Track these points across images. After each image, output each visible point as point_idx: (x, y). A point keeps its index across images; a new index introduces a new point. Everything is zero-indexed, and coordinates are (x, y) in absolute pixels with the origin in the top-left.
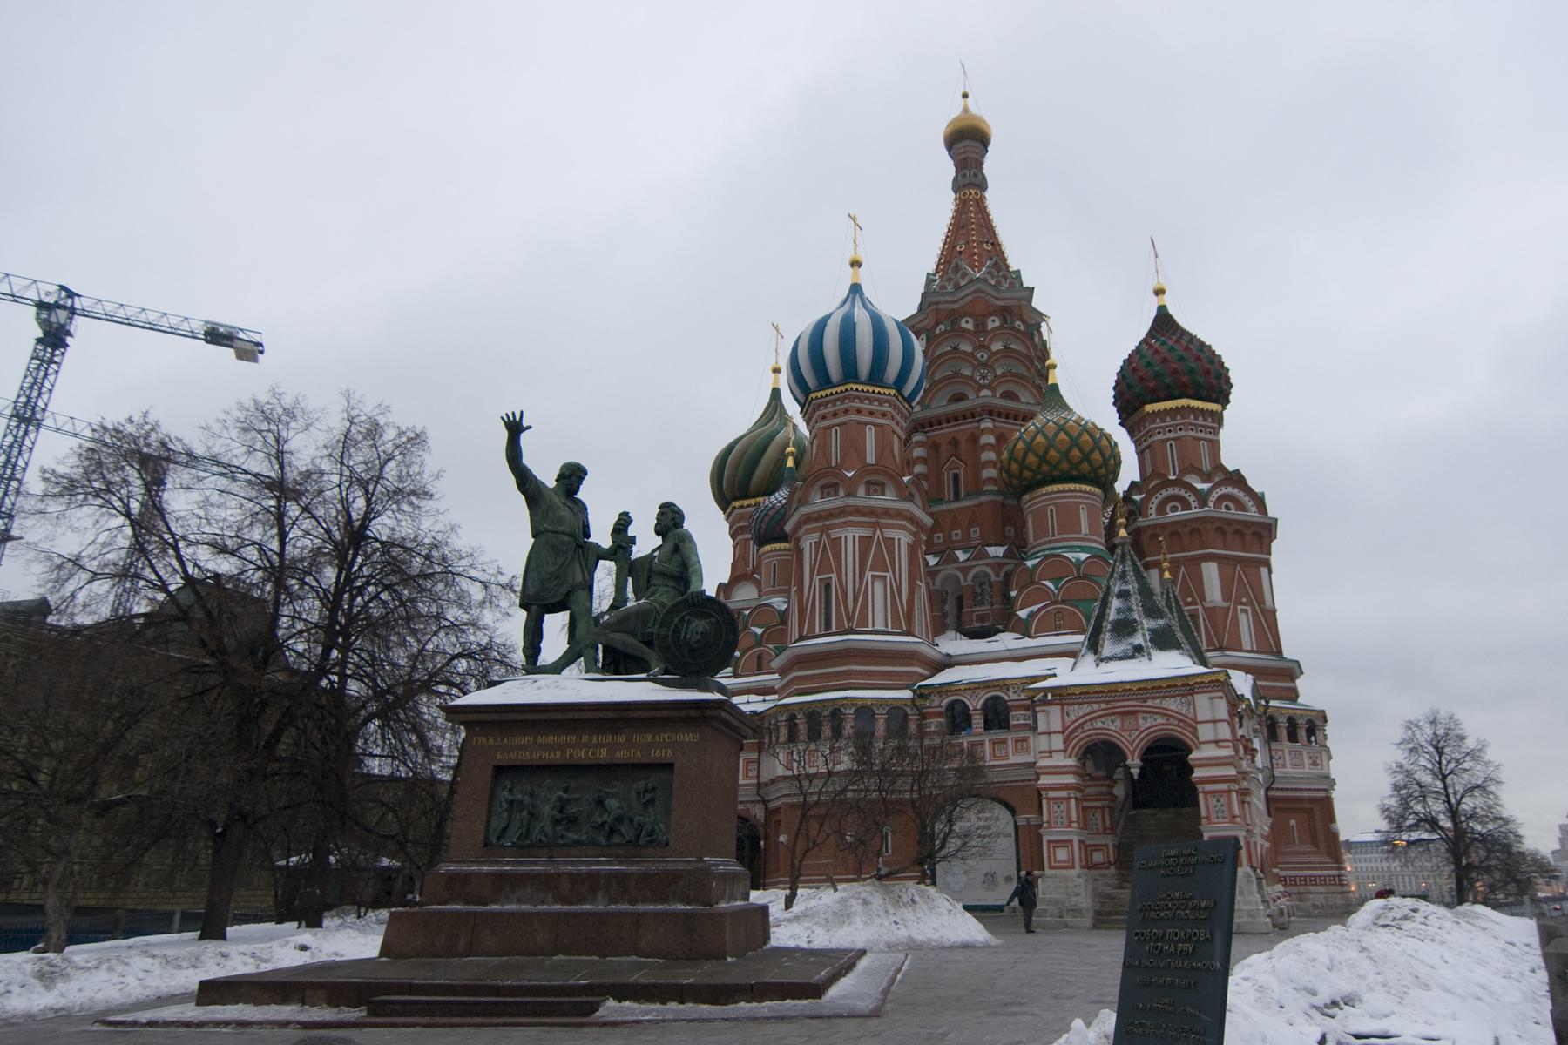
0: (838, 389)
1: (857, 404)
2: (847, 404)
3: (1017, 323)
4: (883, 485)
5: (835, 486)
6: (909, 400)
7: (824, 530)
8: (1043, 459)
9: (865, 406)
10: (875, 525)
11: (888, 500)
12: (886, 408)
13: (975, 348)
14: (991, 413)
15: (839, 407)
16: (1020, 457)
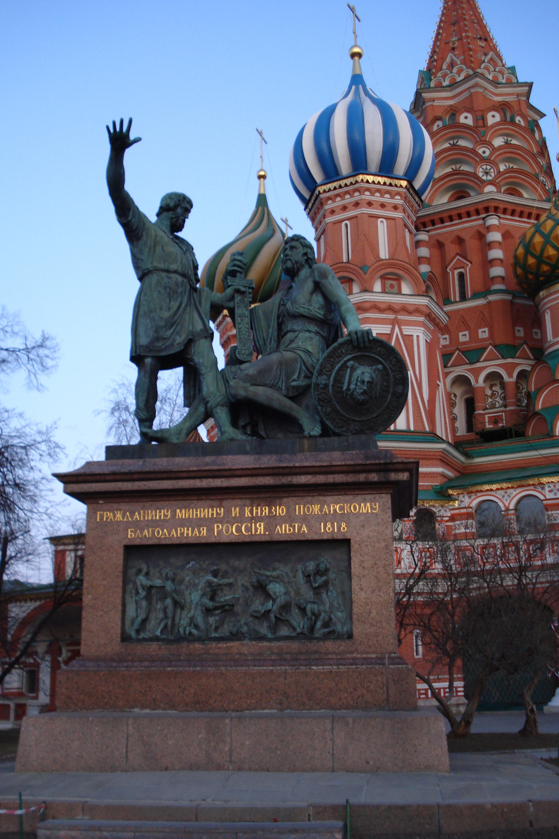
0: (348, 181)
1: (367, 196)
3: (518, 119)
4: (398, 279)
6: (418, 194)
9: (377, 197)
10: (394, 323)
12: (398, 200)
13: (476, 143)
14: (496, 209)
15: (348, 199)
16: (538, 253)
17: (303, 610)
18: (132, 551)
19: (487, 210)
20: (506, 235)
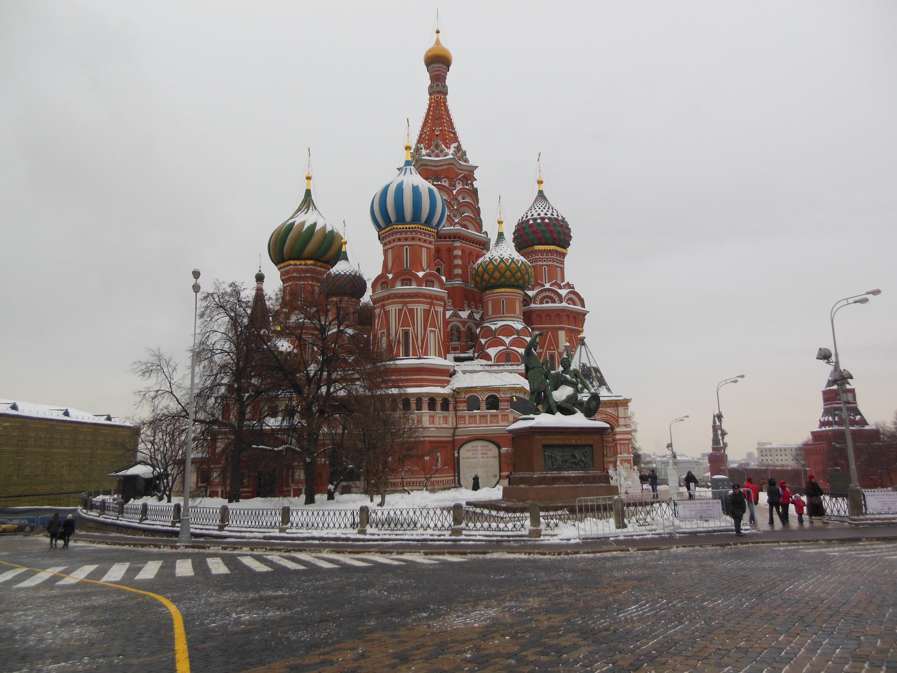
0: (411, 226)
2: (414, 235)
4: (433, 282)
5: (410, 280)
7: (405, 303)
8: (503, 275)
9: (423, 237)
10: (431, 304)
11: (436, 289)
17: (583, 461)
18: (544, 446)
19: (455, 237)
20: (463, 251)
